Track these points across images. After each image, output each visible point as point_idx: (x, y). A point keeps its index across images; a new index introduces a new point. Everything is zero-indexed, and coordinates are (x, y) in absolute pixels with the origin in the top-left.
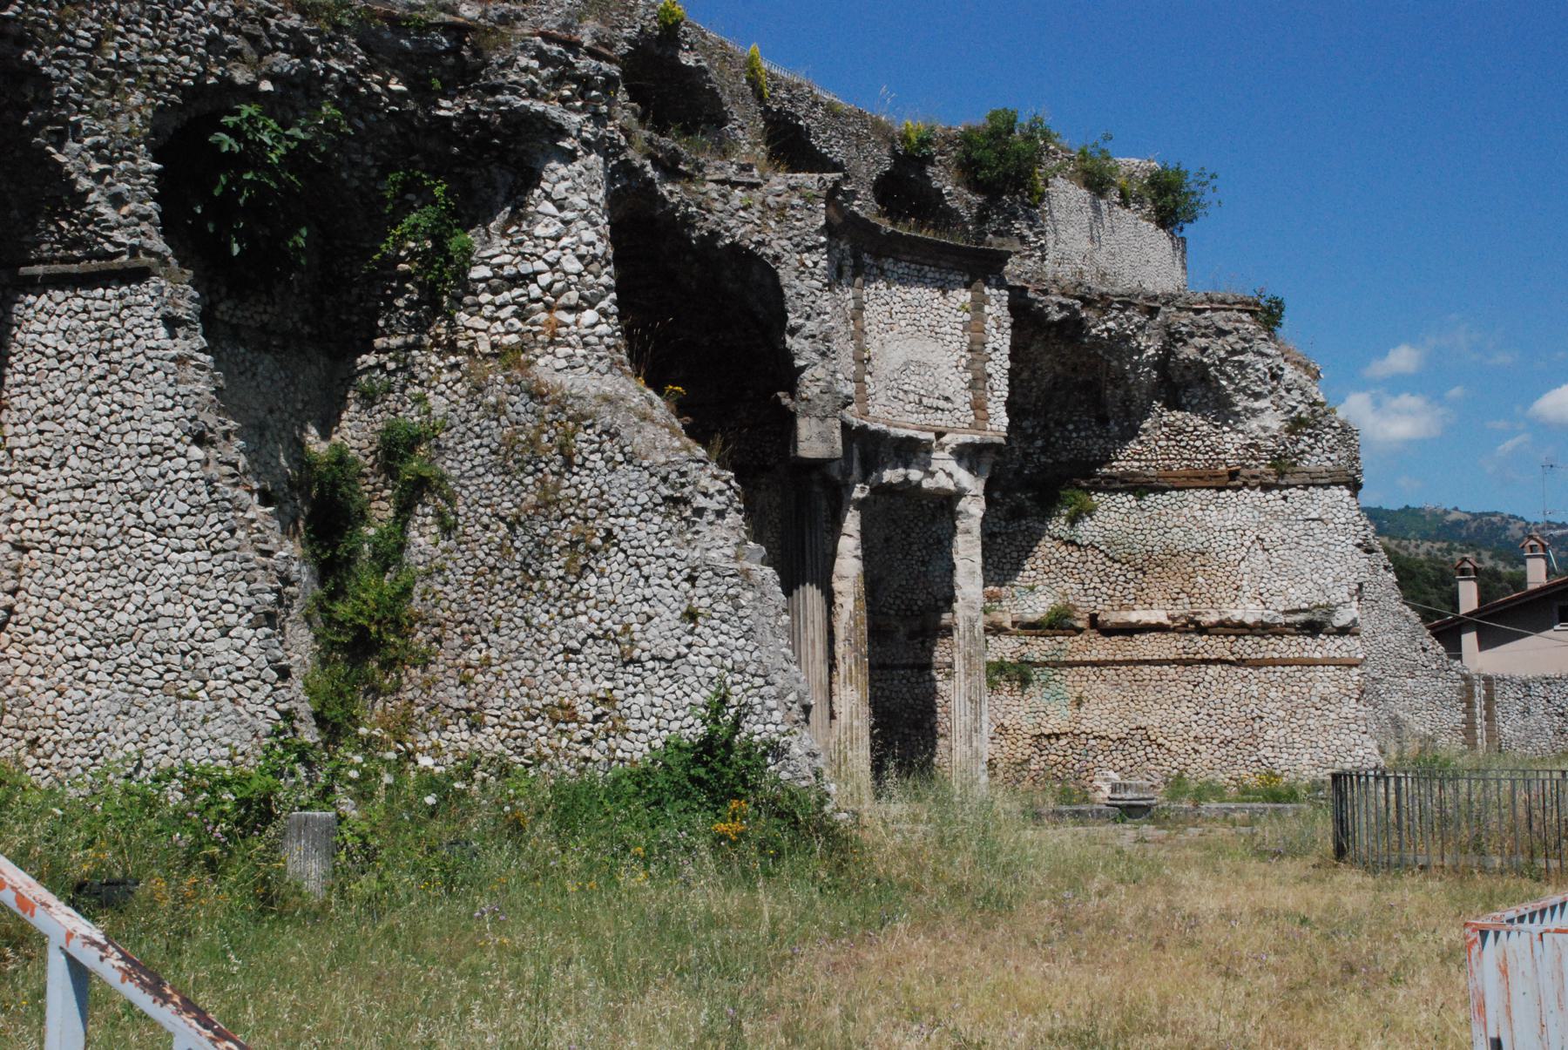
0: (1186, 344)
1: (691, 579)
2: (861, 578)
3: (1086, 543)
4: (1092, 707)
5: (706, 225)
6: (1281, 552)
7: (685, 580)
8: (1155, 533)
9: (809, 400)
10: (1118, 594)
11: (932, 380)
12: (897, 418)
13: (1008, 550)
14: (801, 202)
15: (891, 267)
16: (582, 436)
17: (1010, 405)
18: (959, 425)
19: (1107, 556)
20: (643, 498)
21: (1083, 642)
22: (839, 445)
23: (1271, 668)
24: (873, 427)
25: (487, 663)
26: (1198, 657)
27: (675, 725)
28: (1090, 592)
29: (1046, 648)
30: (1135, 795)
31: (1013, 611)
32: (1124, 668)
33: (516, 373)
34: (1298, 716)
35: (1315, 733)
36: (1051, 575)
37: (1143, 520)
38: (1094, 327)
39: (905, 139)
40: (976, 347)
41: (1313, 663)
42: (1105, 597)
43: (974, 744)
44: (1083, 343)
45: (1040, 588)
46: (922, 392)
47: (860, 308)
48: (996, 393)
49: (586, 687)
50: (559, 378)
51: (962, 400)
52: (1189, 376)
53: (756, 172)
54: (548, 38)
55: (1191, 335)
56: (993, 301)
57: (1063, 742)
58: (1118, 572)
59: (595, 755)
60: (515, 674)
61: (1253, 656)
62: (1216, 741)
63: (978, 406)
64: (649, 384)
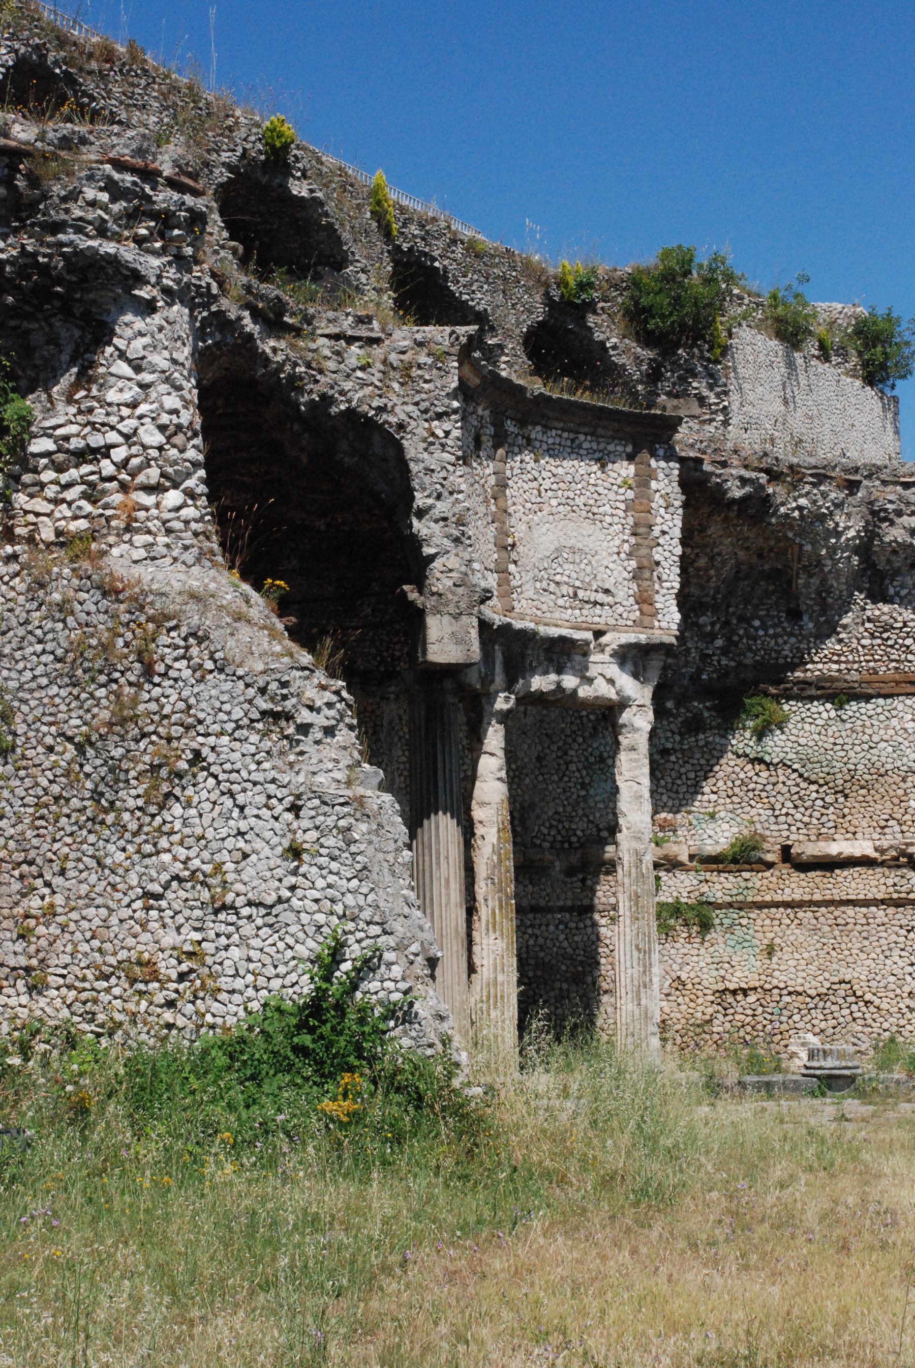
0: (892, 523)
1: (295, 809)
2: (506, 805)
3: (775, 761)
4: (786, 957)
5: (316, 388)
7: (288, 810)
8: (857, 749)
9: (440, 595)
10: (815, 821)
11: (588, 569)
12: (548, 615)
13: (683, 770)
14: (429, 361)
16: (164, 639)
17: (683, 600)
18: (621, 622)
19: (801, 776)
20: (238, 713)
21: (774, 879)
22: (476, 647)
24: (518, 625)
25: (51, 912)
27: (276, 984)
28: (782, 819)
29: (730, 886)
30: (837, 1063)
31: (691, 843)
32: (823, 910)
33: (86, 565)
36: (734, 799)
37: (844, 734)
38: (783, 504)
39: (561, 283)
40: (642, 530)
42: (799, 824)
43: (643, 1002)
44: (769, 524)
45: (722, 814)
46: (577, 584)
47: (502, 485)
48: (665, 584)
49: (169, 939)
50: (137, 570)
51: (625, 592)
52: (897, 562)
53: (375, 324)
54: (119, 165)
55: (899, 514)
56: (661, 476)
57: (752, 998)
58: (814, 795)
59: (181, 1021)
60: (85, 924)
63: (644, 600)
64: (244, 577)
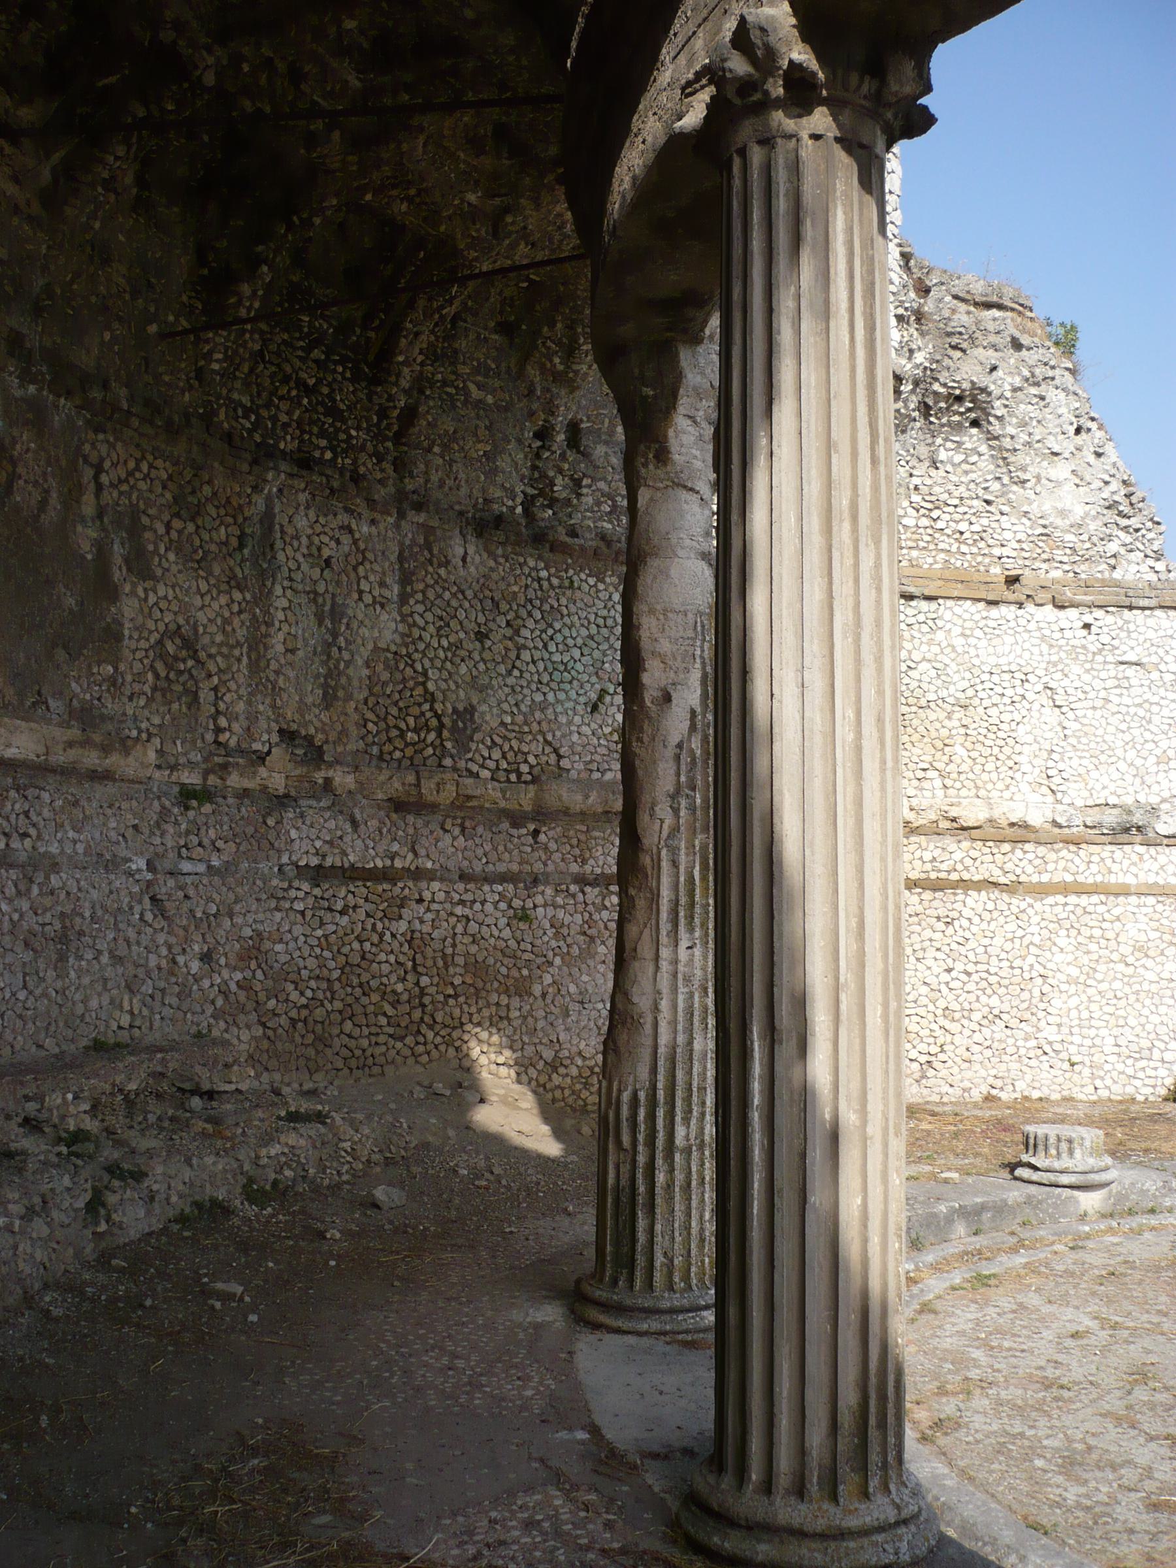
6: (1079, 713)
23: (1060, 899)
26: (954, 876)
30: (1092, 1162)
34: (1099, 976)
35: (1123, 1002)
41: (1123, 891)
61: (1035, 879)
62: (976, 1016)
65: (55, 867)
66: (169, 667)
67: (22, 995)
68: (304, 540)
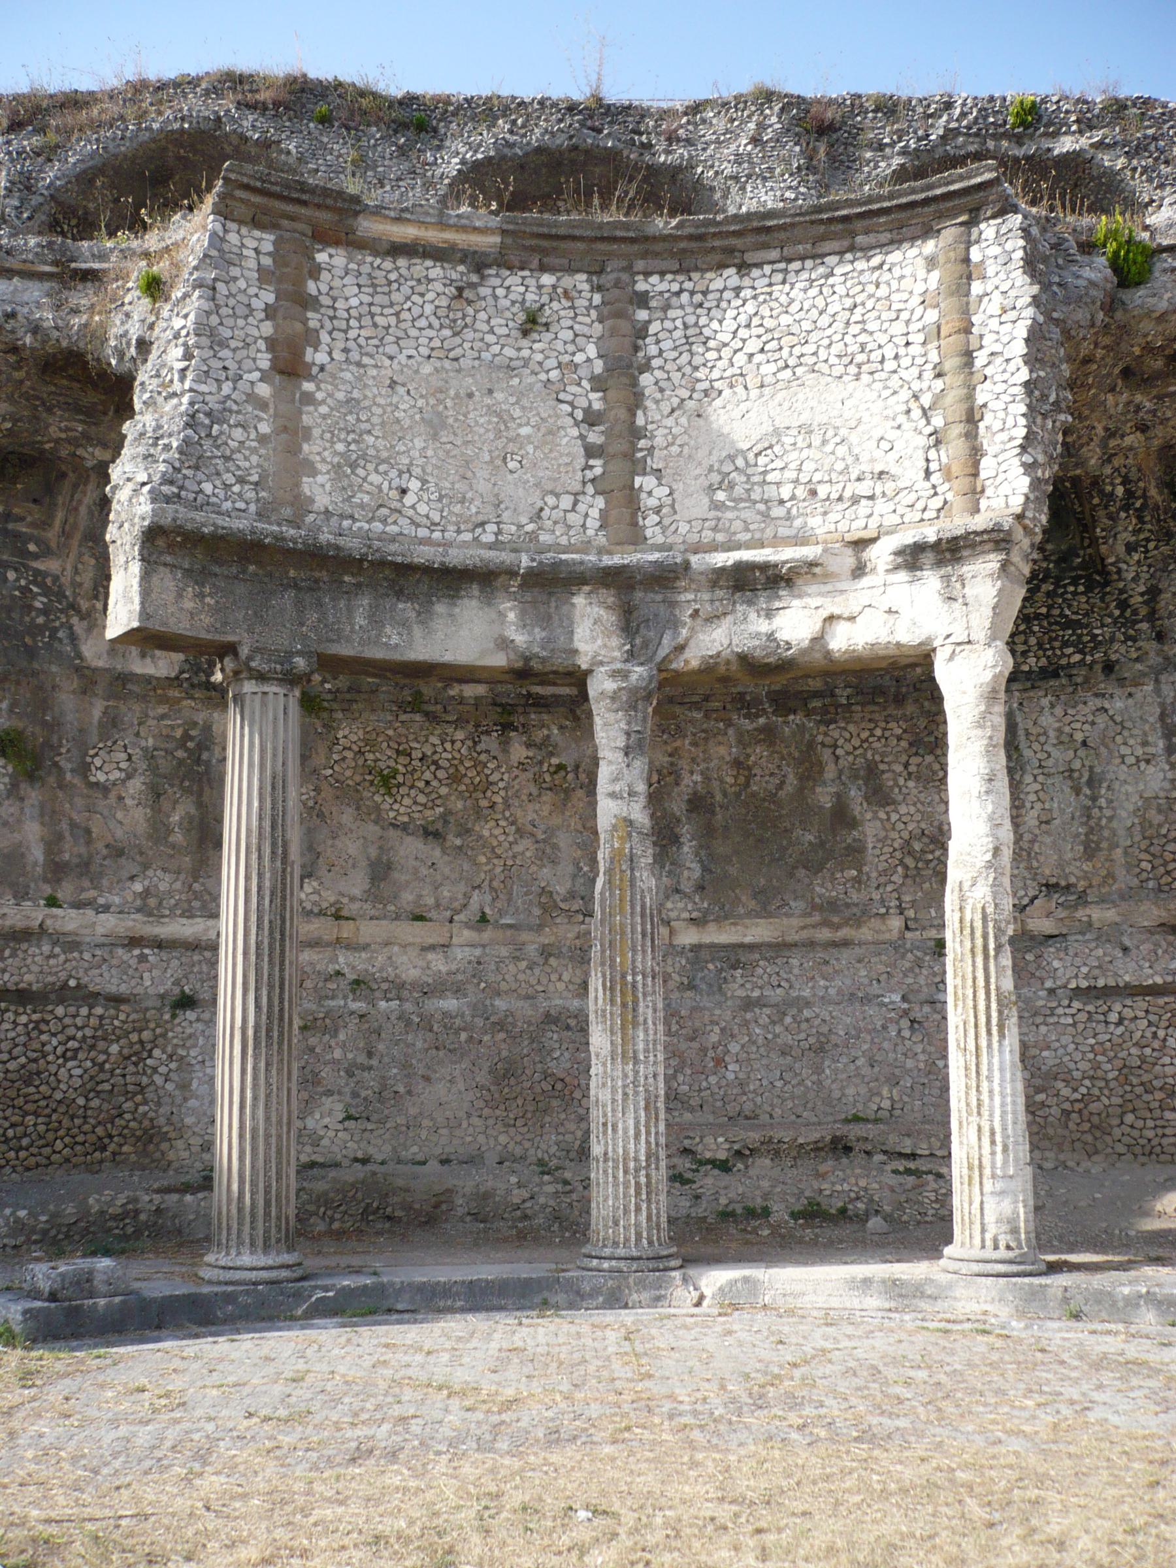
11: (841, 450)
15: (734, 281)
65: (808, 1004)
66: (917, 860)
67: (779, 1084)
68: (1052, 734)
